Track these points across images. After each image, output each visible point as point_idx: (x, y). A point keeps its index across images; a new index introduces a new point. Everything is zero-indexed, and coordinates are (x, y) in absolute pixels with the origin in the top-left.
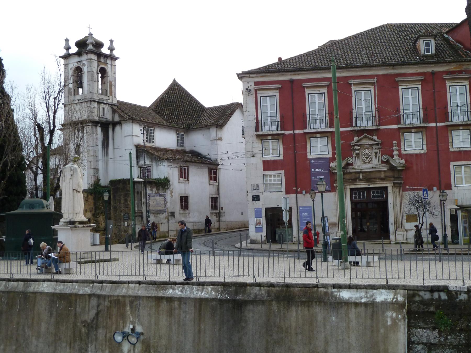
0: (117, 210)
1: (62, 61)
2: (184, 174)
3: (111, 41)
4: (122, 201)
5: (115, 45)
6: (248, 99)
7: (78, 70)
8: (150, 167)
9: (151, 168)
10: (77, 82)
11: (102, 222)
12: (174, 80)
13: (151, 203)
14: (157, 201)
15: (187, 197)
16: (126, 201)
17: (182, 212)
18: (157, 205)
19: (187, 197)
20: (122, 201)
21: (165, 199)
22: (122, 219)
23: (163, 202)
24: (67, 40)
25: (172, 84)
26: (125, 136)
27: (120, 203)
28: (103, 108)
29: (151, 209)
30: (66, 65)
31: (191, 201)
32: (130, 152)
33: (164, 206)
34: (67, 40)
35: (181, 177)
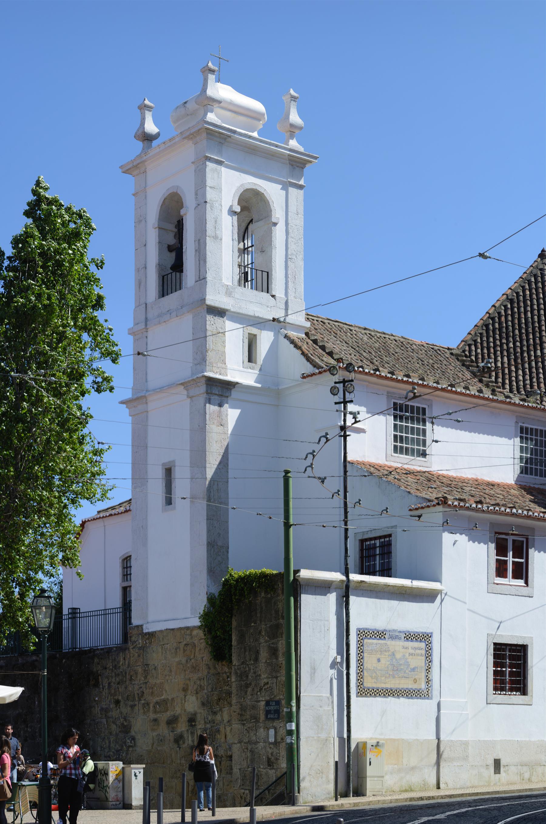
0: (247, 686)
1: (130, 180)
4: (264, 655)
8: (390, 536)
9: (393, 538)
10: (170, 249)
13: (369, 662)
14: (393, 654)
17: (501, 698)
18: (396, 669)
20: (264, 655)
22: (262, 717)
27: (256, 660)
29: (368, 683)
30: (140, 194)
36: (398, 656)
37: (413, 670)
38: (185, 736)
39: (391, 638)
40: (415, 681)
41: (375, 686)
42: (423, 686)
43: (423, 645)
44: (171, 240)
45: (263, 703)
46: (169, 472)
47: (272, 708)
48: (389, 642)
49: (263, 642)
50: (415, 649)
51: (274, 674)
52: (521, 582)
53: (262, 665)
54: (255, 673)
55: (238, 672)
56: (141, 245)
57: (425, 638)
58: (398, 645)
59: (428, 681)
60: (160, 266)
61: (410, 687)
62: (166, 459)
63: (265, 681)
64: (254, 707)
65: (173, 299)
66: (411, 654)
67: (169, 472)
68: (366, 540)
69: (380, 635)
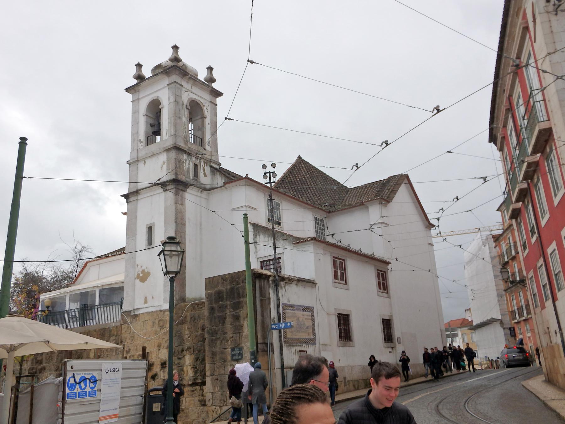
1: (129, 96)
2: (340, 275)
3: (210, 69)
5: (215, 74)
6: (554, 23)
7: (155, 109)
9: (281, 260)
10: (152, 126)
11: (189, 368)
12: (300, 157)
14: (298, 319)
15: (348, 316)
16: (237, 318)
19: (348, 316)
20: (229, 320)
21: (313, 316)
22: (229, 358)
23: (309, 323)
24: (139, 66)
25: (297, 161)
26: (233, 210)
28: (196, 166)
29: (289, 336)
31: (355, 325)
32: (245, 215)
33: (311, 331)
34: (139, 66)
35: (336, 277)
36: (301, 320)
37: (307, 328)
38: (159, 373)
39: (298, 309)
40: (309, 334)
41: (291, 337)
42: (312, 337)
43: (310, 314)
44: (151, 121)
45: (230, 349)
46: (150, 229)
47: (236, 352)
48: (296, 312)
49: (229, 312)
50: (307, 316)
51: (237, 331)
52: (344, 282)
53: (228, 326)
54: (223, 331)
55: (210, 331)
56: (135, 122)
57: (310, 309)
58: (300, 313)
59: (314, 334)
60: (146, 133)
61: (307, 337)
62: (149, 222)
63: (231, 335)
64: (222, 353)
65: (153, 148)
66: (306, 319)
67: (150, 229)
68: (264, 261)
69: (292, 307)
